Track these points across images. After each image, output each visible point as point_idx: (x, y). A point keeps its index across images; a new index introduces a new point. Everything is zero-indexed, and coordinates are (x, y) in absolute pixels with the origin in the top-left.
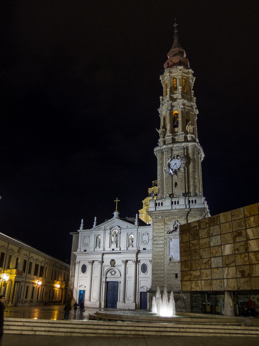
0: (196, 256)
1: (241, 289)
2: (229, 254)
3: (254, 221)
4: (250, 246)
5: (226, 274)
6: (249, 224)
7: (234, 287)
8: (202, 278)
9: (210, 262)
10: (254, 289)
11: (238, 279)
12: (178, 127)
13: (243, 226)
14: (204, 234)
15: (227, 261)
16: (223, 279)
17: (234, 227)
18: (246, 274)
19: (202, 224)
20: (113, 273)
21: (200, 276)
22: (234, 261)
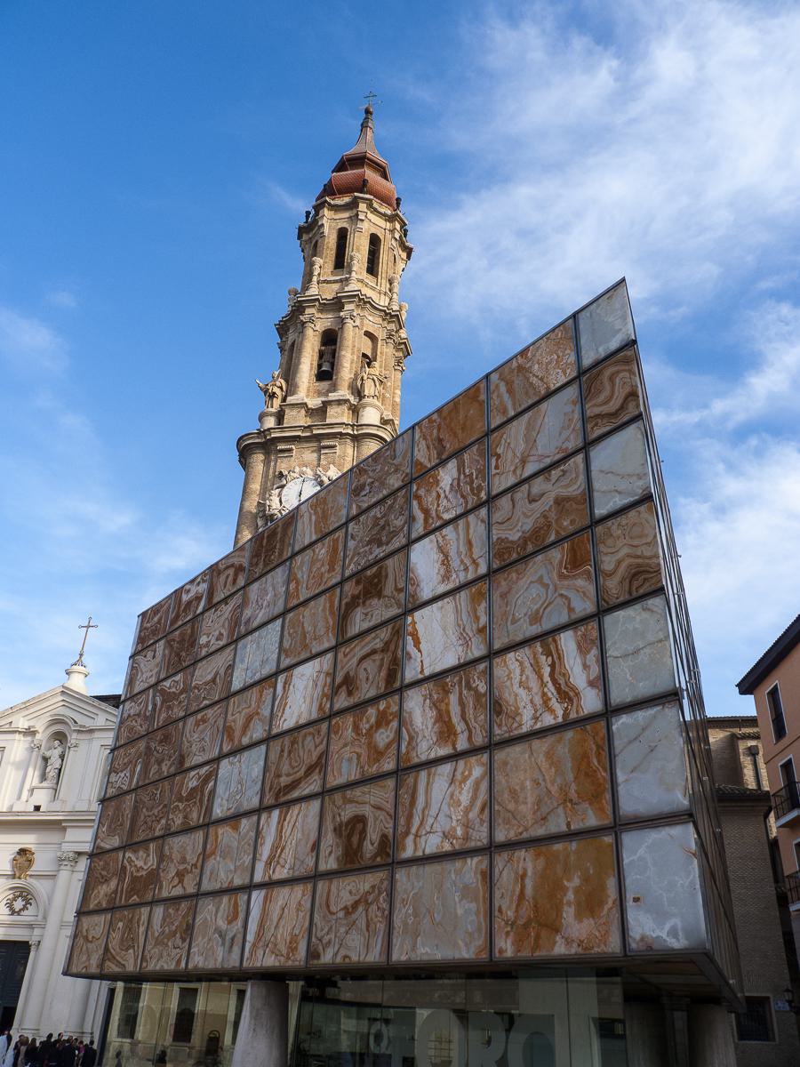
0: (163, 760)
1: (327, 958)
2: (302, 721)
3: (456, 487)
4: (417, 643)
5: (265, 851)
6: (426, 512)
7: (293, 949)
8: (160, 888)
9: (211, 784)
10: (404, 958)
11: (320, 885)
12: (331, 379)
13: (394, 534)
14: (217, 633)
15: (285, 768)
16: (249, 888)
17: (350, 553)
18: (369, 848)
19: (222, 578)
20: (18, 904)
21: (153, 877)
22: (321, 764)
